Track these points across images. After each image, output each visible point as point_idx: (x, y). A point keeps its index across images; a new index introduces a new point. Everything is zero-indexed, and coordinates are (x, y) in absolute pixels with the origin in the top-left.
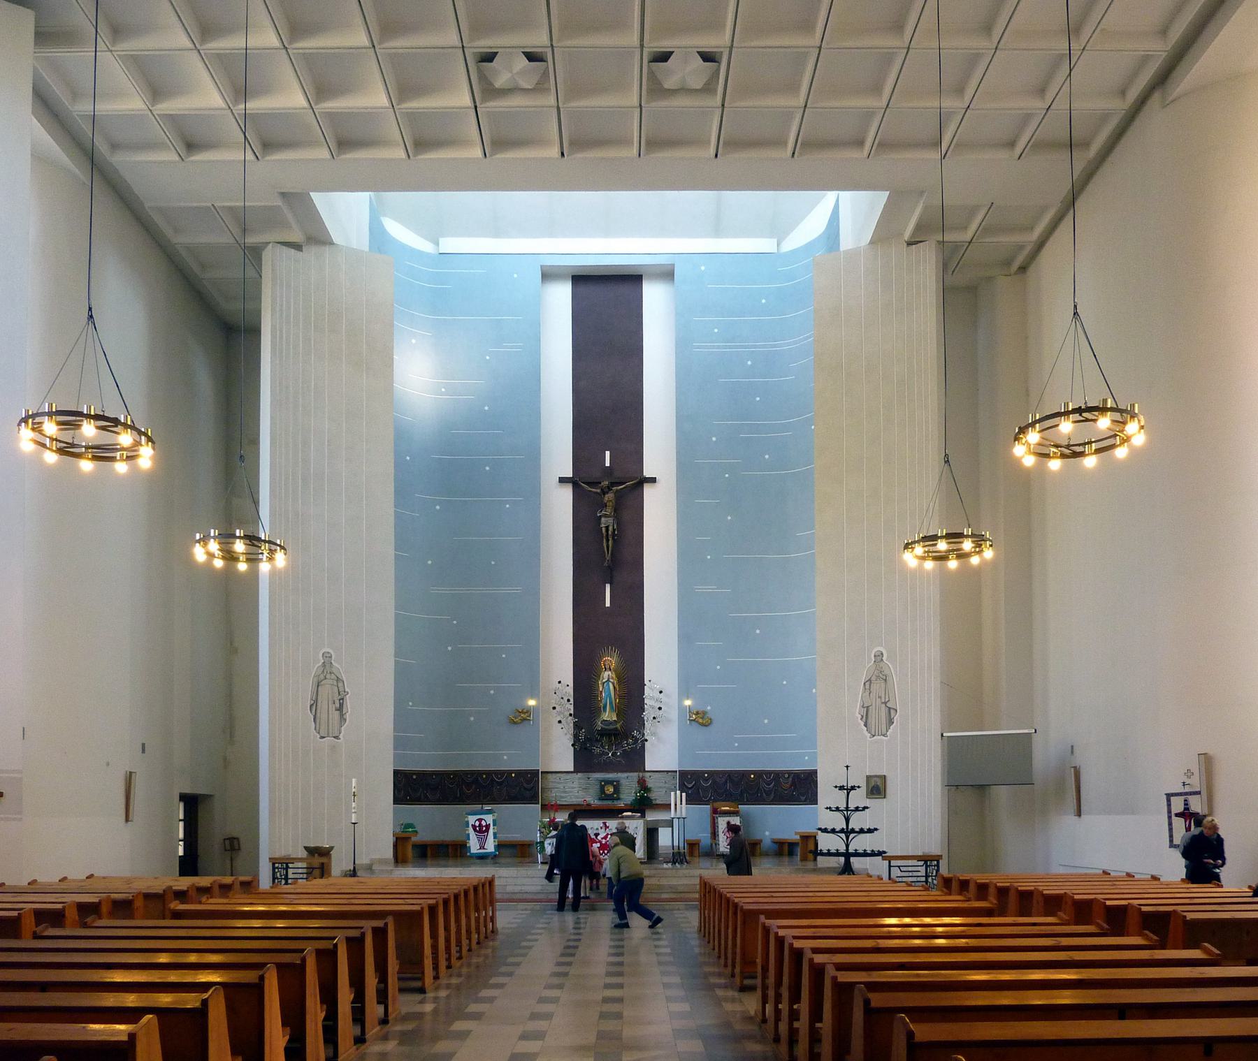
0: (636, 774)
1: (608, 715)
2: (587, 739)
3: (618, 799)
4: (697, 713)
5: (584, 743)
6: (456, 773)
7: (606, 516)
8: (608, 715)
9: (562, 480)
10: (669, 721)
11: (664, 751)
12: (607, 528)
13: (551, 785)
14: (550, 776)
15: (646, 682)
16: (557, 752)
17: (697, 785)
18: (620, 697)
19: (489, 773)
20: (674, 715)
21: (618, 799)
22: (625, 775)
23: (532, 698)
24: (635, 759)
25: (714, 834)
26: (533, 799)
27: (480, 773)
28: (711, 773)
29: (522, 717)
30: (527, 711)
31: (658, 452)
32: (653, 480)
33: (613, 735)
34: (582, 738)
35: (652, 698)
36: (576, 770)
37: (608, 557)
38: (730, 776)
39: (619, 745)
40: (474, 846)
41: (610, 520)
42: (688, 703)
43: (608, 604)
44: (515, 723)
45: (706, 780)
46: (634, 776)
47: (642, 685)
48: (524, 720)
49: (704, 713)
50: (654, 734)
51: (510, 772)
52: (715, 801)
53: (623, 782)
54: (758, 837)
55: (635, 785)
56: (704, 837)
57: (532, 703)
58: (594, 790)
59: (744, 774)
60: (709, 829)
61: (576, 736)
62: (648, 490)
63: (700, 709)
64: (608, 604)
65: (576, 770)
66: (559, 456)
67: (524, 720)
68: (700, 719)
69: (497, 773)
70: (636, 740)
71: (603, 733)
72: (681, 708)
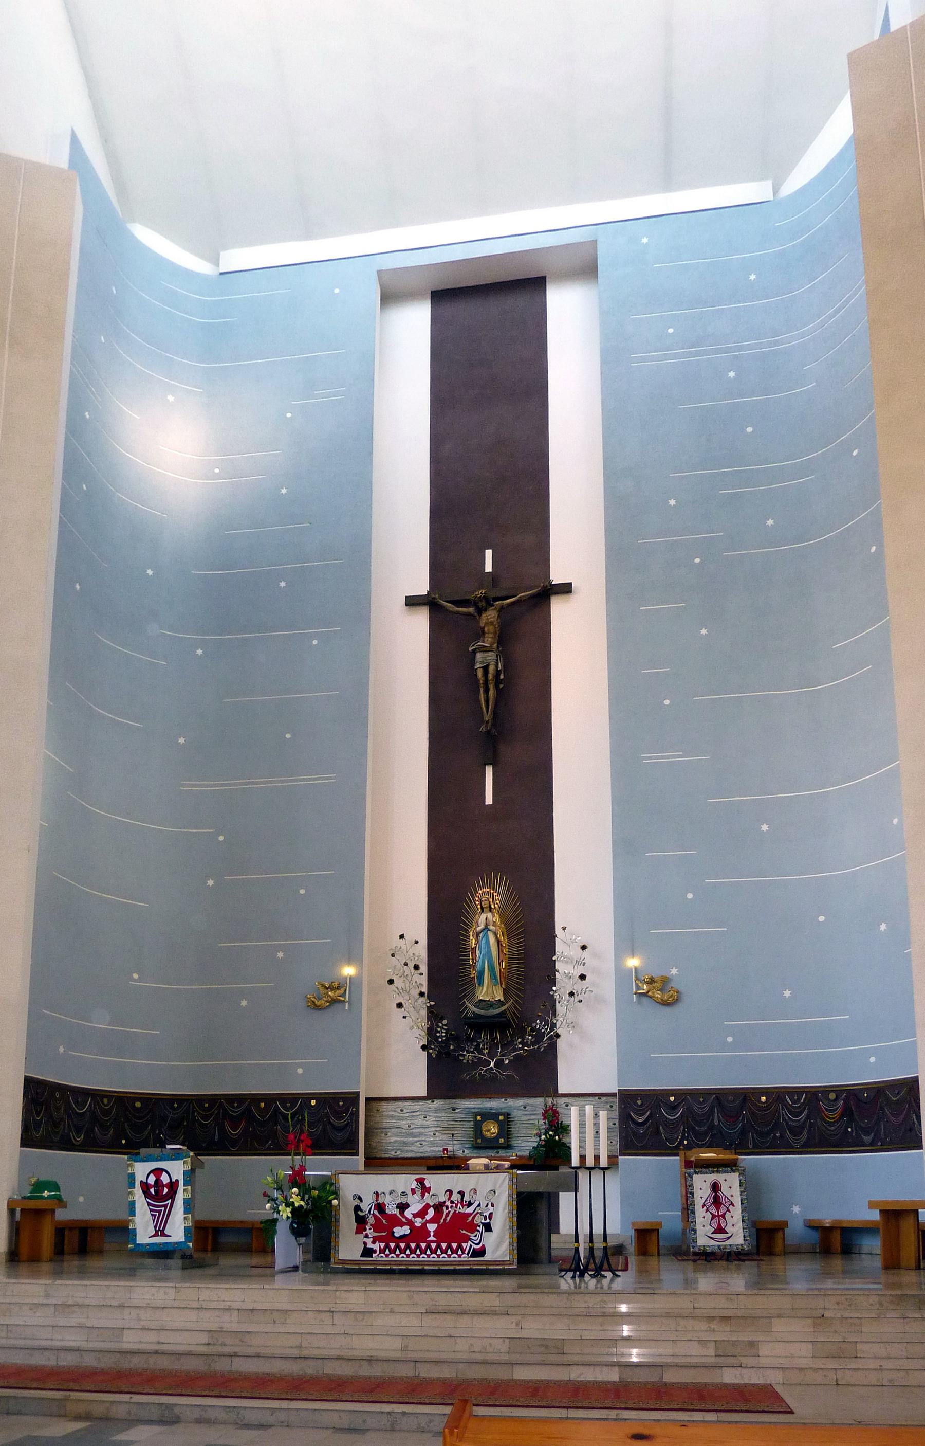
0: (540, 1101)
1: (489, 991)
2: (450, 1037)
3: (508, 1147)
4: (652, 981)
5: (446, 1043)
6: (214, 1099)
7: (484, 649)
8: (489, 991)
9: (412, 602)
11: (592, 1056)
12: (486, 669)
13: (386, 1122)
14: (384, 1106)
15: (558, 930)
16: (394, 1059)
17: (650, 1121)
19: (270, 1099)
20: (604, 986)
21: (508, 1147)
22: (520, 1102)
23: (349, 962)
24: (537, 1070)
25: (688, 1210)
26: (348, 1146)
27: (255, 1099)
28: (683, 1095)
29: (331, 998)
30: (338, 986)
31: (575, 542)
32: (566, 589)
34: (442, 1034)
37: (487, 717)
38: (719, 1099)
39: (507, 1045)
40: (144, 1229)
41: (491, 656)
42: (633, 962)
43: (489, 800)
44: (317, 1008)
45: (673, 1107)
46: (538, 1103)
47: (551, 937)
48: (334, 1001)
49: (665, 980)
50: (573, 1025)
51: (307, 1098)
52: (689, 1148)
53: (515, 1114)
54: (777, 1216)
55: (542, 1123)
56: (669, 1219)
57: (349, 971)
58: (465, 1131)
59: (746, 1096)
60: (679, 1202)
61: (431, 1032)
62: (558, 608)
63: (657, 974)
64: (489, 800)
66: (404, 556)
67: (334, 1001)
68: (657, 992)
69: (285, 1099)
70: (539, 1037)
71: (480, 1025)
72: (621, 974)
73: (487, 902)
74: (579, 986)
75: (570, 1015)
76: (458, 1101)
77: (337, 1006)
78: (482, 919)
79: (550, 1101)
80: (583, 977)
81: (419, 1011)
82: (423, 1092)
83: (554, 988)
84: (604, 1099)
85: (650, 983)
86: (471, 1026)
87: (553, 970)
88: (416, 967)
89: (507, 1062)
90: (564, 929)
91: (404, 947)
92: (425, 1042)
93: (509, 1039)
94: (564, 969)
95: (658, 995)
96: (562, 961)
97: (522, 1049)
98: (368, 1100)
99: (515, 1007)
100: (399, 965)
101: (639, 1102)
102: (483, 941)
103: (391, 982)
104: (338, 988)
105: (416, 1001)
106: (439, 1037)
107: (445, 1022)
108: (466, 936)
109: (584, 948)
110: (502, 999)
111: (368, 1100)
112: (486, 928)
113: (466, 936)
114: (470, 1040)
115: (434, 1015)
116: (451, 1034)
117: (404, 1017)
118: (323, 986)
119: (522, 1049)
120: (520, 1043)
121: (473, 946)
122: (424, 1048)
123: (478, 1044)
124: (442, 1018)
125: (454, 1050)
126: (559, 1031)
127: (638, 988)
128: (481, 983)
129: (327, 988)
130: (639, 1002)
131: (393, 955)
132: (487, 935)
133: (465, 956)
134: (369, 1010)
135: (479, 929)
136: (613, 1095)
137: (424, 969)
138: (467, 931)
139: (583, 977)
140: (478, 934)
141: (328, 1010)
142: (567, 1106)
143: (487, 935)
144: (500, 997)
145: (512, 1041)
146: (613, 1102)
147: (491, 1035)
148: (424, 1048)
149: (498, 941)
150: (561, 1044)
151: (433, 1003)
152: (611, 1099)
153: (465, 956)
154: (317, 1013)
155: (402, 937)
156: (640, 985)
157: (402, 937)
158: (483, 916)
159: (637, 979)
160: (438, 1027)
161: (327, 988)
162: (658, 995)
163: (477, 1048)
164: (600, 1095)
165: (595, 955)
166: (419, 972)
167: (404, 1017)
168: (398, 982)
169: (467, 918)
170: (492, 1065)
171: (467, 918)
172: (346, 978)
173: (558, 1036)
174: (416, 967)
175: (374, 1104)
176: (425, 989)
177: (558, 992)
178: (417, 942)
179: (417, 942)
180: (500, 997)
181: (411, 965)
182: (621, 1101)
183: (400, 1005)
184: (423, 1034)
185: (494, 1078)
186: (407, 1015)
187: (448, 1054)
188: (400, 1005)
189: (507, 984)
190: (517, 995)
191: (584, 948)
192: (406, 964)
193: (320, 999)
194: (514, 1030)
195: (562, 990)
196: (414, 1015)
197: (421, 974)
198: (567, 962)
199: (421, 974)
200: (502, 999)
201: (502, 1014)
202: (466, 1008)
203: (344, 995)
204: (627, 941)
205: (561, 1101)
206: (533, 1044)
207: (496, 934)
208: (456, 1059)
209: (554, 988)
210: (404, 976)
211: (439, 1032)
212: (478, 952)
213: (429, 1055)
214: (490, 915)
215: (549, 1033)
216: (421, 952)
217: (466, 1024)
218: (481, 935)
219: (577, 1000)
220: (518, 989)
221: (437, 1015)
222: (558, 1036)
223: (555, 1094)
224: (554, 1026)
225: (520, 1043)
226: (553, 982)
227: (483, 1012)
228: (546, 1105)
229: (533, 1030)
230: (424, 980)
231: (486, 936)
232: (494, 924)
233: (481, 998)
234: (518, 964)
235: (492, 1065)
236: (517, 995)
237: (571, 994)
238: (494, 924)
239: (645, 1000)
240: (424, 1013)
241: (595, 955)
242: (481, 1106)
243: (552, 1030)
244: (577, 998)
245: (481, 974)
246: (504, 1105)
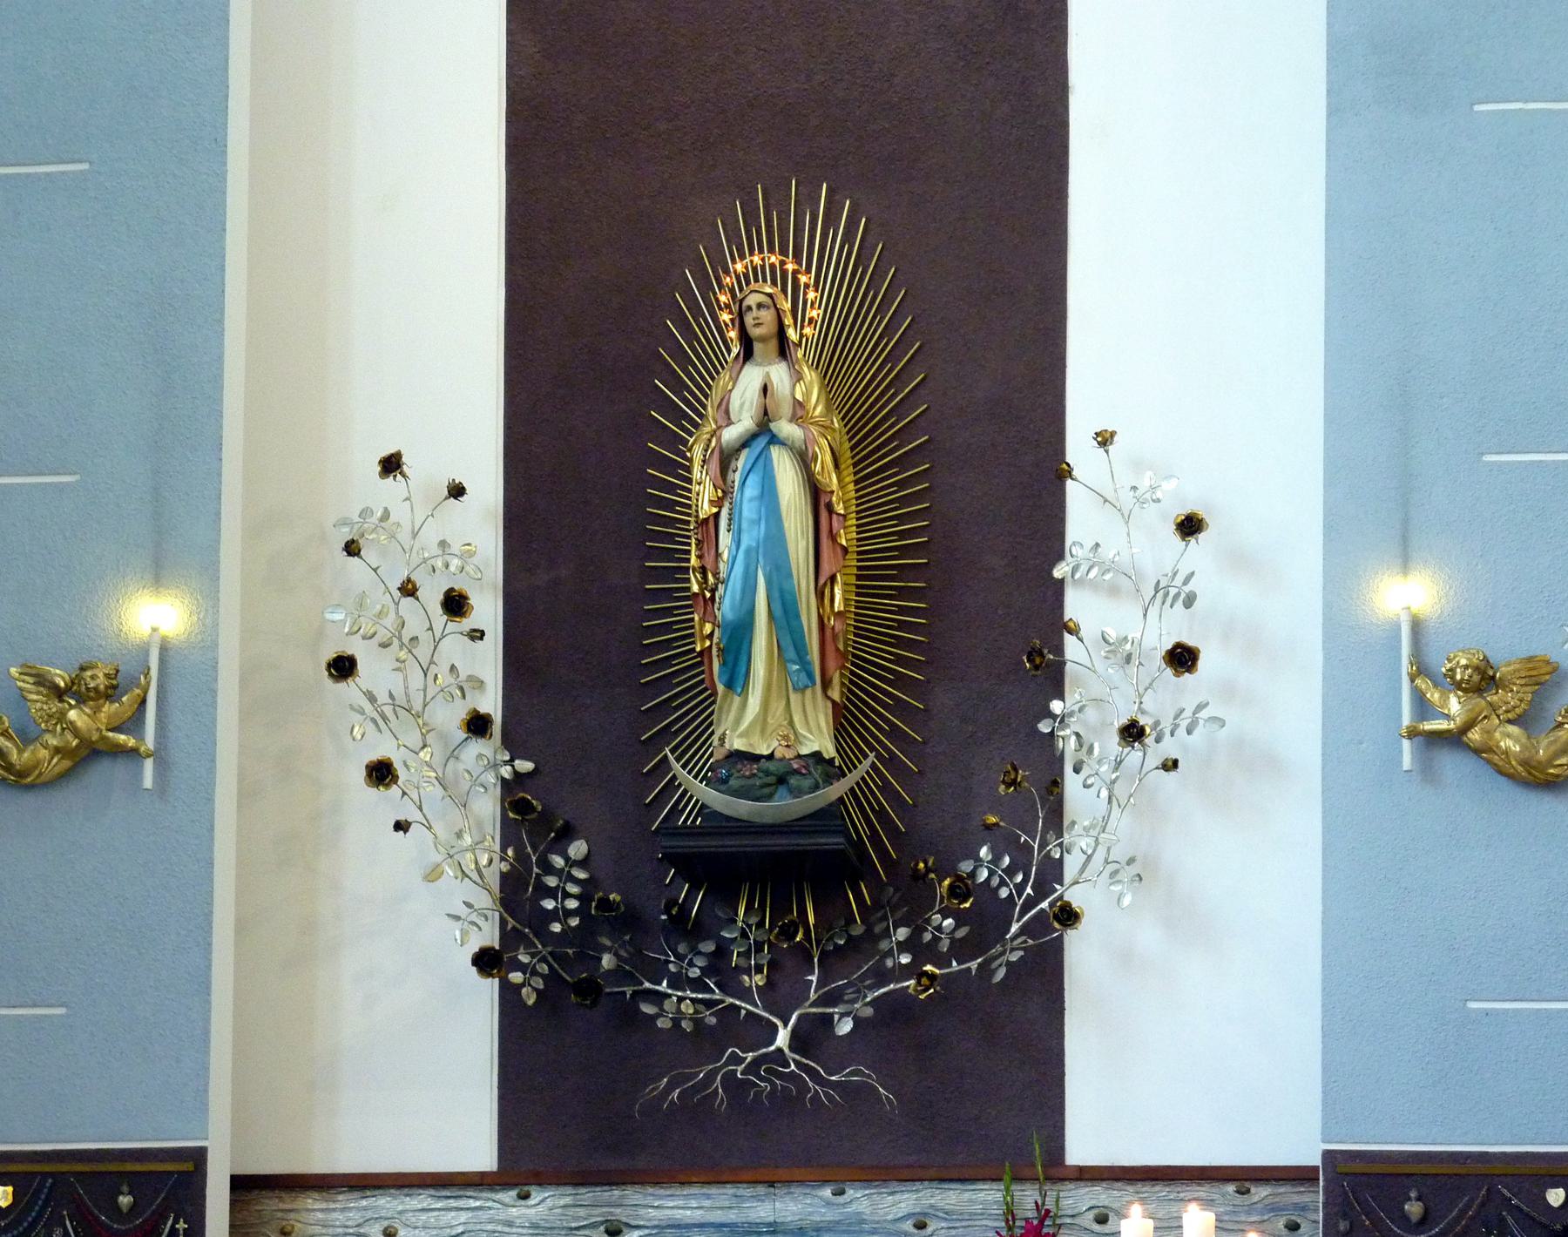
0: (988, 1196)
1: (772, 716)
2: (602, 917)
4: (1484, 680)
5: (584, 940)
10: (1258, 762)
14: (313, 1211)
15: (1078, 448)
18: (867, 582)
20: (1277, 700)
23: (159, 575)
29: (88, 735)
33: (811, 874)
34: (564, 904)
35: (1118, 581)
36: (518, 1168)
42: (1406, 594)
47: (1053, 474)
50: (1136, 871)
57: (152, 615)
61: (517, 894)
63: (1506, 653)
65: (518, 1168)
70: (986, 921)
71: (731, 865)
72: (1347, 640)
73: (767, 316)
74: (1165, 697)
75: (1121, 822)
76: (633, 1195)
77: (102, 771)
78: (743, 391)
79: (1027, 1198)
80: (1182, 658)
81: (464, 799)
82: (482, 1155)
83: (1056, 706)
84: (1260, 1192)
85: (1478, 690)
86: (693, 867)
87: (1057, 626)
88: (455, 604)
89: (845, 1027)
90: (1104, 440)
91: (400, 513)
92: (488, 935)
93: (858, 929)
94: (1102, 620)
95: (1510, 741)
96: (1095, 586)
97: (913, 970)
98: (242, 1185)
99: (886, 788)
100: (382, 598)
101: (1414, 1209)
102: (751, 490)
103: (343, 667)
104: (111, 693)
105: (453, 755)
106: (553, 915)
107: (578, 849)
108: (671, 467)
109: (1190, 526)
110: (829, 751)
111: (242, 1185)
112: (763, 430)
113: (671, 467)
114: (684, 928)
115: (529, 817)
116: (604, 904)
117: (401, 826)
118: (41, 680)
119: (913, 970)
120: (903, 947)
121: (706, 510)
122: (486, 961)
123: (722, 952)
124: (567, 834)
125: (618, 975)
126: (1075, 896)
127: (1423, 707)
128: (737, 679)
129: (59, 694)
130: (1426, 770)
131: (352, 549)
132: (766, 468)
133: (668, 554)
134: (247, 795)
135: (730, 435)
136: (1300, 1176)
137: (488, 610)
138: (677, 443)
139: (1182, 658)
140: (726, 459)
141: (69, 798)
142: (1102, 1220)
143: (766, 468)
144: (818, 739)
145: (871, 937)
146: (1303, 1208)
147: (780, 909)
148: (486, 961)
149: (816, 492)
150: (1082, 953)
151: (525, 766)
152: (1290, 1195)
153: (668, 554)
154: (29, 800)
155: (391, 465)
156: (1434, 696)
157: (391, 465)
158: (752, 377)
159: (1420, 669)
160: (548, 869)
161: (59, 694)
162: (1510, 741)
163: (719, 966)
164: (1244, 1177)
165: (1239, 561)
166: (467, 623)
167: (401, 826)
168: (374, 671)
169: (678, 387)
170: (782, 1038)
171: (678, 387)
172: (144, 650)
173: (1068, 916)
174: (455, 604)
175: (270, 1204)
176: (491, 703)
177: (1074, 724)
178: (457, 491)
179: (457, 491)
180: (818, 739)
181: (432, 595)
182: (1338, 1206)
183: (381, 773)
184: (484, 900)
185: (790, 1101)
186: (411, 814)
187: (590, 989)
188: (381, 773)
189: (853, 685)
190: (894, 734)
191: (1190, 526)
192: (409, 589)
193: (26, 738)
194: (877, 886)
195: (1091, 714)
196: (445, 820)
197: (477, 635)
198: (1113, 591)
199: (477, 635)
200: (829, 751)
201: (828, 817)
202: (672, 785)
203: (134, 722)
204: (1378, 500)
205: (1078, 1200)
206: (961, 950)
207: (804, 460)
208: (627, 1015)
209: (1056, 706)
210: (398, 641)
211: (551, 893)
212: (725, 539)
213: (509, 995)
214: (779, 374)
215: (1030, 904)
216: (477, 537)
217: (671, 859)
218: (742, 462)
219: (1154, 760)
220: (900, 708)
221: (546, 818)
222: (1068, 916)
223: (1056, 1170)
224: (1052, 872)
225: (903, 947)
226: (1053, 679)
227: (742, 808)
228: (1010, 1214)
229: (962, 888)
230: (487, 661)
231: (763, 464)
232: (799, 412)
233: (738, 744)
234: (902, 593)
235: (782, 1038)
236: (894, 734)
237: (1132, 733)
238: (799, 412)
239: (1451, 764)
240: (488, 807)
241: (1239, 561)
242: (732, 1216)
243: (1042, 890)
244: (1156, 752)
245: (741, 632)
246: (830, 1215)
